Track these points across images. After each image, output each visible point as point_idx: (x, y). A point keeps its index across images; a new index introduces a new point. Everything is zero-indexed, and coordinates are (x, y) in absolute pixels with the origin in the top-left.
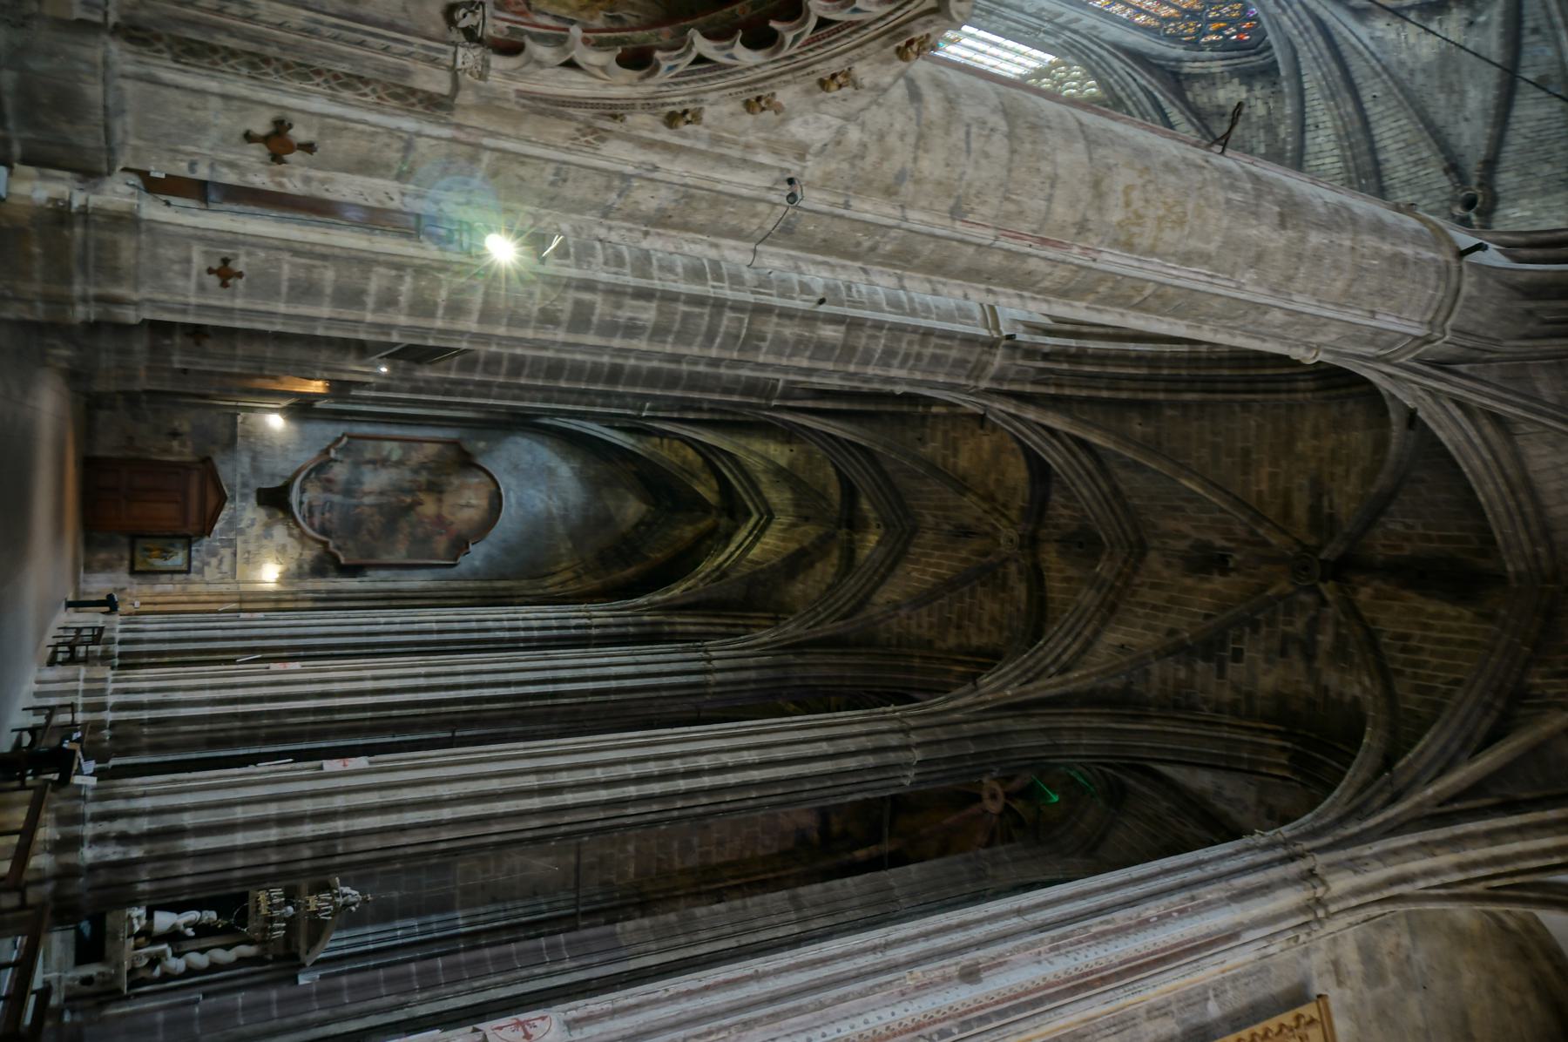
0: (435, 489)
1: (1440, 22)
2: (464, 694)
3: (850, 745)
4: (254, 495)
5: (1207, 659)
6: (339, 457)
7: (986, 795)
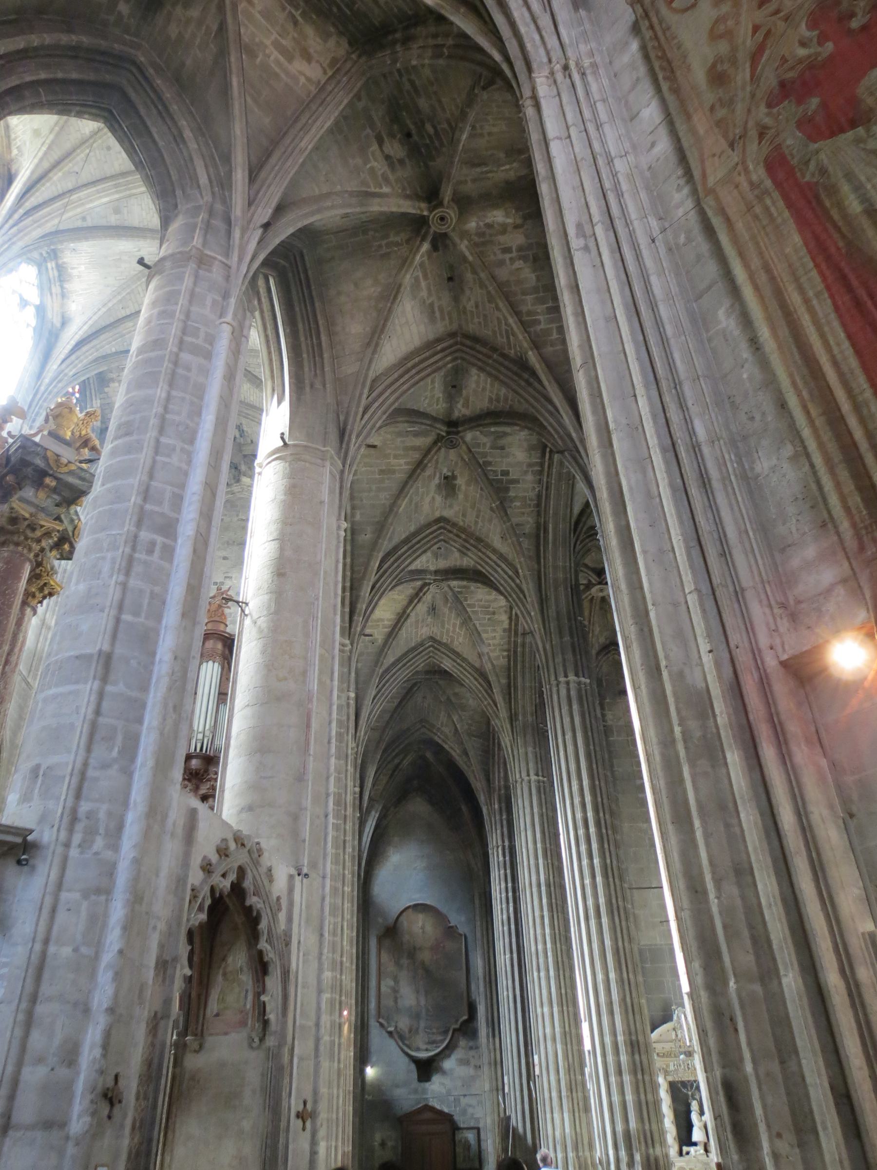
0: (412, 953)
1: (72, 268)
2: (549, 945)
3: (567, 720)
4: (422, 1084)
5: (507, 490)
6: (393, 1024)
7: (601, 594)
